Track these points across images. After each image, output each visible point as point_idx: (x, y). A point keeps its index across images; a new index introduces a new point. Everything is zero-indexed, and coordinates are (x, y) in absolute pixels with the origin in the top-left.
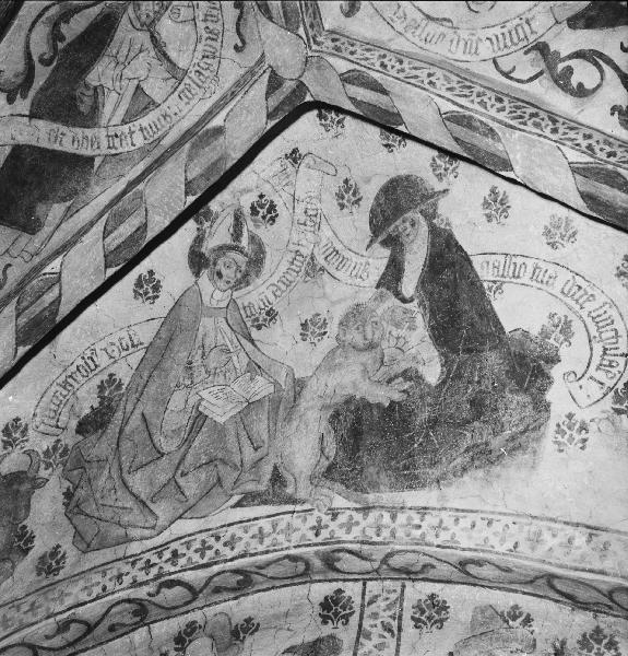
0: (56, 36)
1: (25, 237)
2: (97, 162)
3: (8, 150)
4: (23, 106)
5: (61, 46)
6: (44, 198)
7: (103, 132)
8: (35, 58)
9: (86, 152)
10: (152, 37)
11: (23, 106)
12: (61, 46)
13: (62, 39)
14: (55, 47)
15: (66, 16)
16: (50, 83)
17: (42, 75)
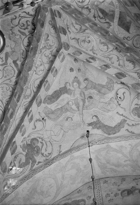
0: (102, 18)
1: (132, 23)
2: (120, 11)
3: (119, 26)
4: (112, 23)
5: (103, 17)
6: (126, 20)
7: (116, 10)
8: (105, 22)
9: (119, 13)
10: (102, 2)
11: (112, 23)
12: (103, 17)
13: (102, 17)
14: (104, 18)
15: (99, 17)
16: (109, 19)
17: (107, 21)
